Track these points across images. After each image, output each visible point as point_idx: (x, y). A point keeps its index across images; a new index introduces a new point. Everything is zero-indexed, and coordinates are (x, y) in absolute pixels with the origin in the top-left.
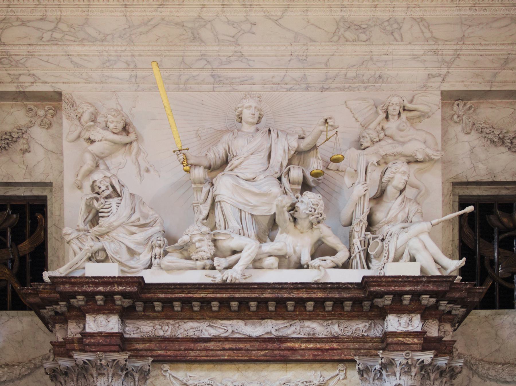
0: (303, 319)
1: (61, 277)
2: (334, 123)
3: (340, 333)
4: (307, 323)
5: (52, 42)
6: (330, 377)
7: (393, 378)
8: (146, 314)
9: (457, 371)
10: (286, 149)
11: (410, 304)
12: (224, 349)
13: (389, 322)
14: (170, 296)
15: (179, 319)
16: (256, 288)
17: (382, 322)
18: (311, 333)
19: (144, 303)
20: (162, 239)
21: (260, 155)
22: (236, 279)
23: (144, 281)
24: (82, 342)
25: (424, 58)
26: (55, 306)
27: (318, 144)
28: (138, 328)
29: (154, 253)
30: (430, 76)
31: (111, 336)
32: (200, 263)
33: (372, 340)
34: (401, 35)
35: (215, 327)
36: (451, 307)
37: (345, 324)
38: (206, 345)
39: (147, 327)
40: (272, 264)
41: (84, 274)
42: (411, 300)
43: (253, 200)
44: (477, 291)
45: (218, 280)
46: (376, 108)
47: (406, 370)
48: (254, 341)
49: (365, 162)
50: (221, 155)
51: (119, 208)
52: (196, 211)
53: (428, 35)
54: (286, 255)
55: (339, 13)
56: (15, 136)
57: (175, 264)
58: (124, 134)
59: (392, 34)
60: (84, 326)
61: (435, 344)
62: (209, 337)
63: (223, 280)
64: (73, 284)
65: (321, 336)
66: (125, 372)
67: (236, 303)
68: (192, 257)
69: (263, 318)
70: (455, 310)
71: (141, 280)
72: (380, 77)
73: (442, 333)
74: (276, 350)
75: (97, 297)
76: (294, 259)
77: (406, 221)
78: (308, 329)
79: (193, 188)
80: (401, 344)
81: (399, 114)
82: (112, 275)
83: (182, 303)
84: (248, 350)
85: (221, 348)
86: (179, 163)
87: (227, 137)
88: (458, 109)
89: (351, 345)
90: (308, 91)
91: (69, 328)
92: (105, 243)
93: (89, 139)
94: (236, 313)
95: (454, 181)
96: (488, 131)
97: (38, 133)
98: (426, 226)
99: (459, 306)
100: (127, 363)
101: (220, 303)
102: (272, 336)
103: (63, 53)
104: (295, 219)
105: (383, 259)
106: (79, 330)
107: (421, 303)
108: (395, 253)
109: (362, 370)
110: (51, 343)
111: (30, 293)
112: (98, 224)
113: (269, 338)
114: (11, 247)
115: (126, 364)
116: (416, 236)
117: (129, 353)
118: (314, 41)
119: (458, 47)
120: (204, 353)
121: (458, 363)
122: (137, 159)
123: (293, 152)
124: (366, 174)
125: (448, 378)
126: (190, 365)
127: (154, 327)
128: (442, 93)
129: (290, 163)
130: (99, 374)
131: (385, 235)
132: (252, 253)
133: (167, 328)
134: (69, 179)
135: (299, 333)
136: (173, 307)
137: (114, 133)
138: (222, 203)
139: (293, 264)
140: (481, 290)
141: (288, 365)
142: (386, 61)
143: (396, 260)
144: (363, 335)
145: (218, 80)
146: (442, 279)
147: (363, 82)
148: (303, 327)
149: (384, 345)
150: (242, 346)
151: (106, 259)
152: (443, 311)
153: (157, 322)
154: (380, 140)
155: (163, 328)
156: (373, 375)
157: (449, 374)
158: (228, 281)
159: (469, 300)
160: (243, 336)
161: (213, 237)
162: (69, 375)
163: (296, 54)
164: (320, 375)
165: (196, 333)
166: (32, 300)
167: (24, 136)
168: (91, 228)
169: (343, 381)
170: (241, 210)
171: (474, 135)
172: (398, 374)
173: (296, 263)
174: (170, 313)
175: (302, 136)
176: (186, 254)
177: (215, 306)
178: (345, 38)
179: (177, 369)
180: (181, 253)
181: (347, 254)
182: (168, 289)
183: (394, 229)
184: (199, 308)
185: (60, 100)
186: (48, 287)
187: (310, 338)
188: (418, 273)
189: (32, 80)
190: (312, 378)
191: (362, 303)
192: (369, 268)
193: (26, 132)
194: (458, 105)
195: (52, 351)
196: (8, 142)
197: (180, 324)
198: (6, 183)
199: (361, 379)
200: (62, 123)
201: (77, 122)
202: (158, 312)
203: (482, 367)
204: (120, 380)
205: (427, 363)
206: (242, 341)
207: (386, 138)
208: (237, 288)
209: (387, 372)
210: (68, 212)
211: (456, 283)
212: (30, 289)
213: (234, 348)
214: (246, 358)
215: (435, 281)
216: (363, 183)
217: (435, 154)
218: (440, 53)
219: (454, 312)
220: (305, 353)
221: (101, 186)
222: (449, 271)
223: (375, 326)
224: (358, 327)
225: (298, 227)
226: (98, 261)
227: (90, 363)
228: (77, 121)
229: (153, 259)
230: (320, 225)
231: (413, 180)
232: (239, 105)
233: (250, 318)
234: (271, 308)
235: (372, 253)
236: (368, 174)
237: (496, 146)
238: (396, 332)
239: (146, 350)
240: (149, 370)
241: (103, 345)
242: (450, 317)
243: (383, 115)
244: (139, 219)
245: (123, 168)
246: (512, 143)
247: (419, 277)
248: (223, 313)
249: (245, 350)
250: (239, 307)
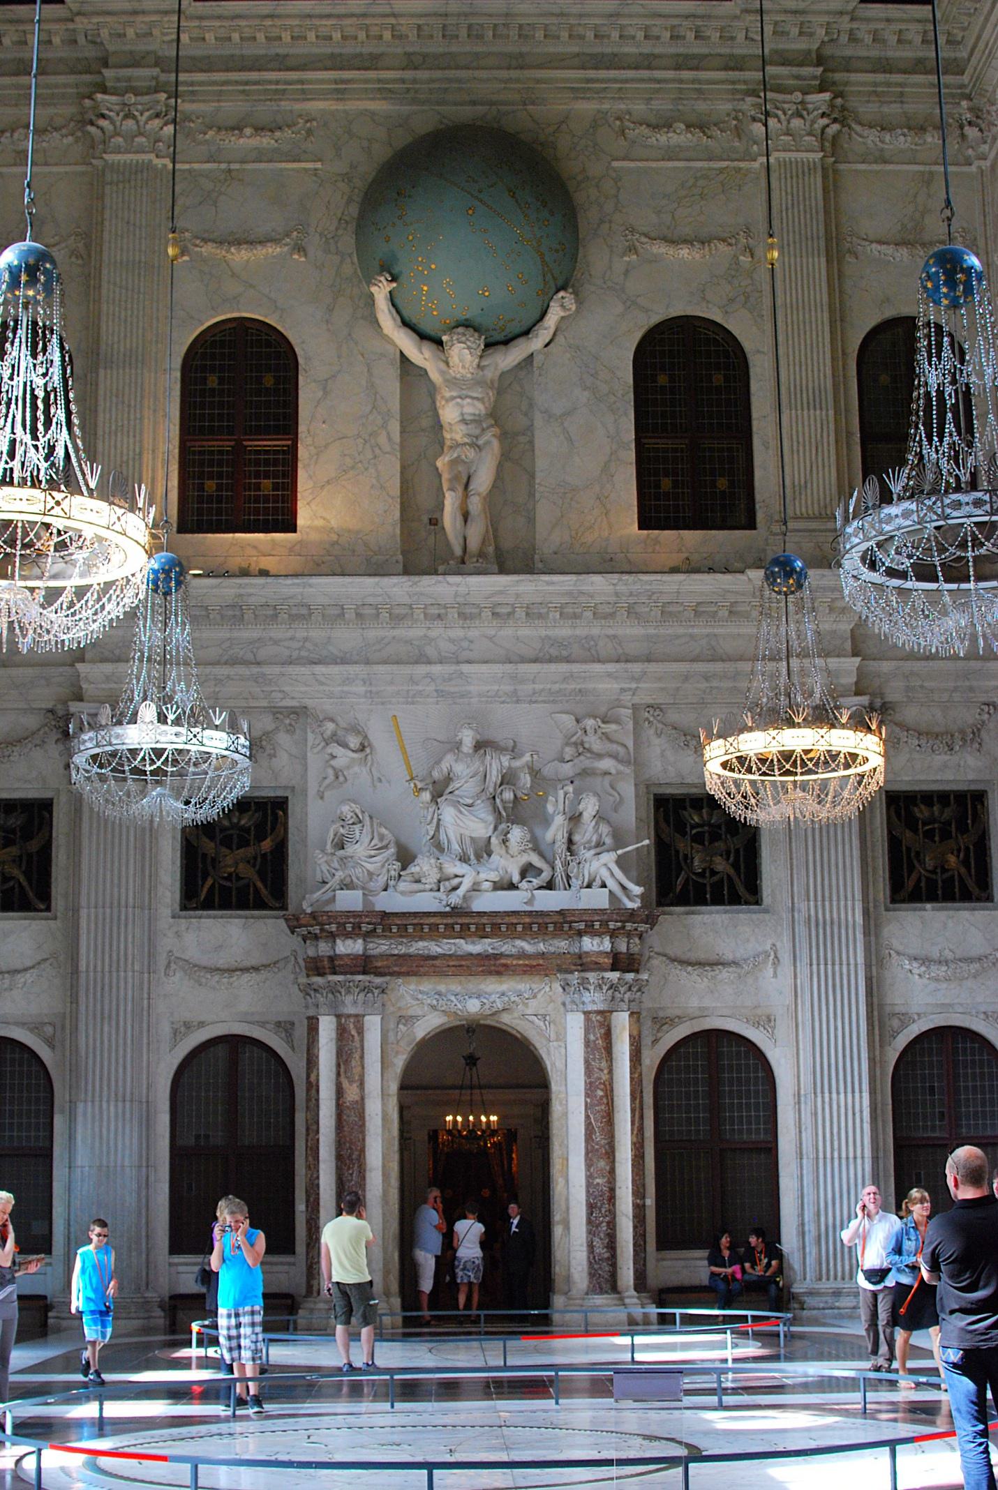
32: (428, 887)
224: (561, 945)
233: (470, 936)
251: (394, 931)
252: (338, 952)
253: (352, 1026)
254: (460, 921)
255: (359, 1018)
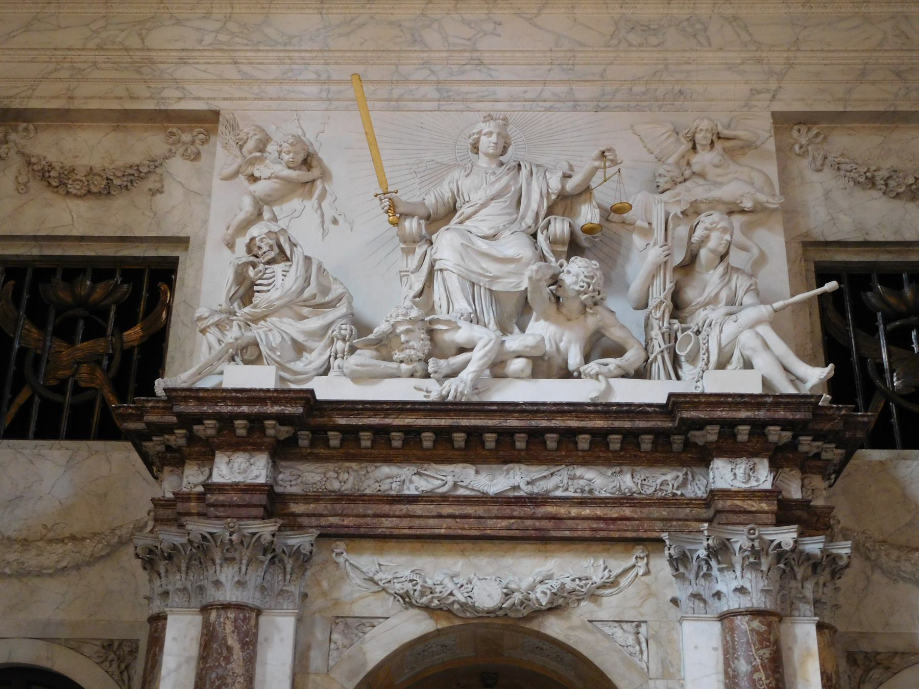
0: (572, 464)
1: (183, 390)
2: (616, 156)
3: (634, 489)
4: (579, 471)
5: (215, 46)
6: (620, 570)
7: (729, 575)
8: (316, 451)
9: (842, 563)
10: (544, 191)
11: (749, 441)
12: (440, 516)
13: (716, 472)
14: (354, 421)
15: (368, 461)
16: (495, 411)
17: (705, 470)
18: (587, 488)
19: (313, 432)
20: (348, 327)
21: (506, 201)
22: (462, 393)
23: (314, 396)
24: (205, 499)
25: (742, 67)
26: (167, 437)
27: (593, 185)
28: (299, 476)
29: (333, 350)
30: (754, 92)
31: (253, 490)
33: (690, 503)
34: (708, 39)
35: (427, 475)
36: (818, 447)
37: (642, 473)
38: (410, 507)
39: (313, 474)
40: (522, 371)
41: (221, 383)
42: (751, 434)
43: (494, 268)
44: (860, 419)
45: (434, 397)
46: (678, 134)
47: (752, 560)
48: (491, 502)
49: (663, 211)
50: (446, 200)
51: (286, 279)
52: (404, 284)
53: (746, 38)
54: (545, 354)
55: (619, 10)
56: (144, 170)
57: (365, 368)
58: (304, 168)
59: (694, 36)
60: (211, 470)
61: (799, 513)
62: (417, 493)
63: (442, 396)
64: (201, 400)
65: (604, 494)
66: (269, 556)
67: (463, 435)
68: (395, 357)
69: (506, 462)
70: (826, 451)
71: (309, 396)
72: (681, 92)
73: (810, 492)
74: (527, 518)
75: (237, 422)
76: (558, 361)
77: (731, 302)
78: (582, 482)
79: (402, 249)
80: (740, 512)
81: (712, 142)
82: (265, 386)
83: (374, 434)
84: (480, 517)
85: (435, 514)
86: (382, 211)
87: (456, 174)
88: (801, 137)
89: (655, 512)
90: (577, 111)
91: (185, 474)
92: (258, 331)
93: (253, 175)
94: (463, 453)
95: (806, 239)
96: (848, 167)
97: (178, 166)
98: (764, 310)
99: (833, 446)
100: (275, 539)
101: (436, 435)
102: (522, 494)
103: (230, 61)
104: (558, 298)
105: (701, 364)
106: (201, 479)
107: (767, 439)
108: (719, 355)
109: (676, 559)
110: (153, 500)
111: (131, 414)
112: (251, 303)
113: (516, 497)
114: (113, 335)
115: (272, 542)
116: (752, 327)
117: (280, 522)
118: (583, 45)
119: (791, 54)
120: (406, 522)
121: (843, 549)
122: (320, 206)
123: (554, 197)
124: (666, 230)
125: (828, 578)
126: (380, 544)
127: (325, 474)
128: (774, 114)
129: (550, 211)
130: (226, 560)
131: (700, 325)
132: (489, 351)
133: (346, 476)
134: (216, 232)
135: (567, 489)
136: (358, 440)
137: (289, 168)
138: (445, 272)
139: (555, 370)
140: (866, 419)
141: (548, 546)
142: (688, 72)
143: (722, 365)
144: (674, 495)
145: (446, 95)
146: (799, 400)
147: (656, 100)
148: (572, 478)
149: (710, 513)
150: (469, 510)
151: (258, 359)
152: (807, 453)
153: (331, 466)
154: (685, 180)
155: (341, 477)
156: (696, 568)
157: (828, 570)
158: (450, 398)
159: (848, 435)
160: (473, 493)
161: (428, 325)
162: (175, 559)
163: (559, 62)
164: (603, 566)
165: (394, 485)
166: (131, 425)
167: (157, 170)
168: (240, 308)
169: (643, 578)
170: (473, 284)
171: (828, 173)
172: (738, 568)
173: (561, 368)
174: (353, 451)
175: (569, 172)
176: (384, 351)
177: (428, 440)
178: (627, 41)
179: (359, 552)
180: (377, 350)
181: (643, 355)
182: (353, 410)
183: (715, 314)
184: (401, 442)
185: (216, 121)
186: (160, 405)
187: (585, 498)
188: (758, 390)
189: (181, 95)
190: (590, 572)
191: (669, 438)
192: (678, 378)
193: (161, 164)
194: (799, 131)
195: (152, 514)
196: (132, 178)
197: (369, 470)
198: (121, 237)
199: (674, 576)
200: (215, 153)
201: (238, 153)
202: (334, 448)
203: (887, 555)
204: (260, 569)
205: (788, 548)
206: (471, 501)
207: (695, 176)
208: (465, 410)
209: (719, 563)
210: (207, 283)
211: (822, 407)
212: (132, 408)
213: (457, 513)
214: (476, 533)
215: (788, 403)
216: (661, 244)
217: (770, 200)
218: (765, 61)
219: (825, 456)
220: (577, 524)
221: (262, 245)
222: (809, 385)
223: (693, 477)
224: (664, 480)
225: (564, 310)
226: (246, 362)
227: (213, 537)
228: (237, 150)
229: (332, 359)
230: (599, 308)
231: (739, 237)
232: (475, 131)
234: (520, 444)
235: (682, 353)
236: (670, 232)
237: (864, 189)
238: (729, 491)
239: (308, 515)
240: (311, 553)
241: (239, 506)
242: (819, 463)
243: (685, 146)
244: (314, 296)
245: (299, 220)
246: (886, 185)
247: (760, 396)
248: (440, 452)
249: (475, 518)
250: (467, 442)
251: (334, 442)
252: (216, 479)
253: (229, 627)
254: (464, 422)
255: (248, 616)
